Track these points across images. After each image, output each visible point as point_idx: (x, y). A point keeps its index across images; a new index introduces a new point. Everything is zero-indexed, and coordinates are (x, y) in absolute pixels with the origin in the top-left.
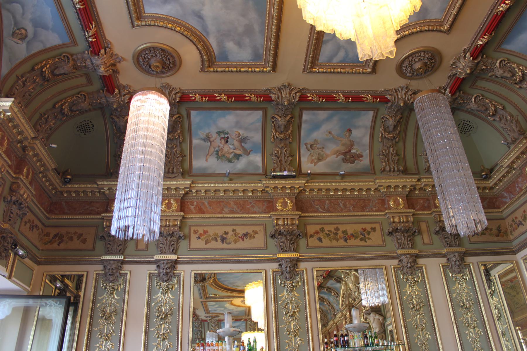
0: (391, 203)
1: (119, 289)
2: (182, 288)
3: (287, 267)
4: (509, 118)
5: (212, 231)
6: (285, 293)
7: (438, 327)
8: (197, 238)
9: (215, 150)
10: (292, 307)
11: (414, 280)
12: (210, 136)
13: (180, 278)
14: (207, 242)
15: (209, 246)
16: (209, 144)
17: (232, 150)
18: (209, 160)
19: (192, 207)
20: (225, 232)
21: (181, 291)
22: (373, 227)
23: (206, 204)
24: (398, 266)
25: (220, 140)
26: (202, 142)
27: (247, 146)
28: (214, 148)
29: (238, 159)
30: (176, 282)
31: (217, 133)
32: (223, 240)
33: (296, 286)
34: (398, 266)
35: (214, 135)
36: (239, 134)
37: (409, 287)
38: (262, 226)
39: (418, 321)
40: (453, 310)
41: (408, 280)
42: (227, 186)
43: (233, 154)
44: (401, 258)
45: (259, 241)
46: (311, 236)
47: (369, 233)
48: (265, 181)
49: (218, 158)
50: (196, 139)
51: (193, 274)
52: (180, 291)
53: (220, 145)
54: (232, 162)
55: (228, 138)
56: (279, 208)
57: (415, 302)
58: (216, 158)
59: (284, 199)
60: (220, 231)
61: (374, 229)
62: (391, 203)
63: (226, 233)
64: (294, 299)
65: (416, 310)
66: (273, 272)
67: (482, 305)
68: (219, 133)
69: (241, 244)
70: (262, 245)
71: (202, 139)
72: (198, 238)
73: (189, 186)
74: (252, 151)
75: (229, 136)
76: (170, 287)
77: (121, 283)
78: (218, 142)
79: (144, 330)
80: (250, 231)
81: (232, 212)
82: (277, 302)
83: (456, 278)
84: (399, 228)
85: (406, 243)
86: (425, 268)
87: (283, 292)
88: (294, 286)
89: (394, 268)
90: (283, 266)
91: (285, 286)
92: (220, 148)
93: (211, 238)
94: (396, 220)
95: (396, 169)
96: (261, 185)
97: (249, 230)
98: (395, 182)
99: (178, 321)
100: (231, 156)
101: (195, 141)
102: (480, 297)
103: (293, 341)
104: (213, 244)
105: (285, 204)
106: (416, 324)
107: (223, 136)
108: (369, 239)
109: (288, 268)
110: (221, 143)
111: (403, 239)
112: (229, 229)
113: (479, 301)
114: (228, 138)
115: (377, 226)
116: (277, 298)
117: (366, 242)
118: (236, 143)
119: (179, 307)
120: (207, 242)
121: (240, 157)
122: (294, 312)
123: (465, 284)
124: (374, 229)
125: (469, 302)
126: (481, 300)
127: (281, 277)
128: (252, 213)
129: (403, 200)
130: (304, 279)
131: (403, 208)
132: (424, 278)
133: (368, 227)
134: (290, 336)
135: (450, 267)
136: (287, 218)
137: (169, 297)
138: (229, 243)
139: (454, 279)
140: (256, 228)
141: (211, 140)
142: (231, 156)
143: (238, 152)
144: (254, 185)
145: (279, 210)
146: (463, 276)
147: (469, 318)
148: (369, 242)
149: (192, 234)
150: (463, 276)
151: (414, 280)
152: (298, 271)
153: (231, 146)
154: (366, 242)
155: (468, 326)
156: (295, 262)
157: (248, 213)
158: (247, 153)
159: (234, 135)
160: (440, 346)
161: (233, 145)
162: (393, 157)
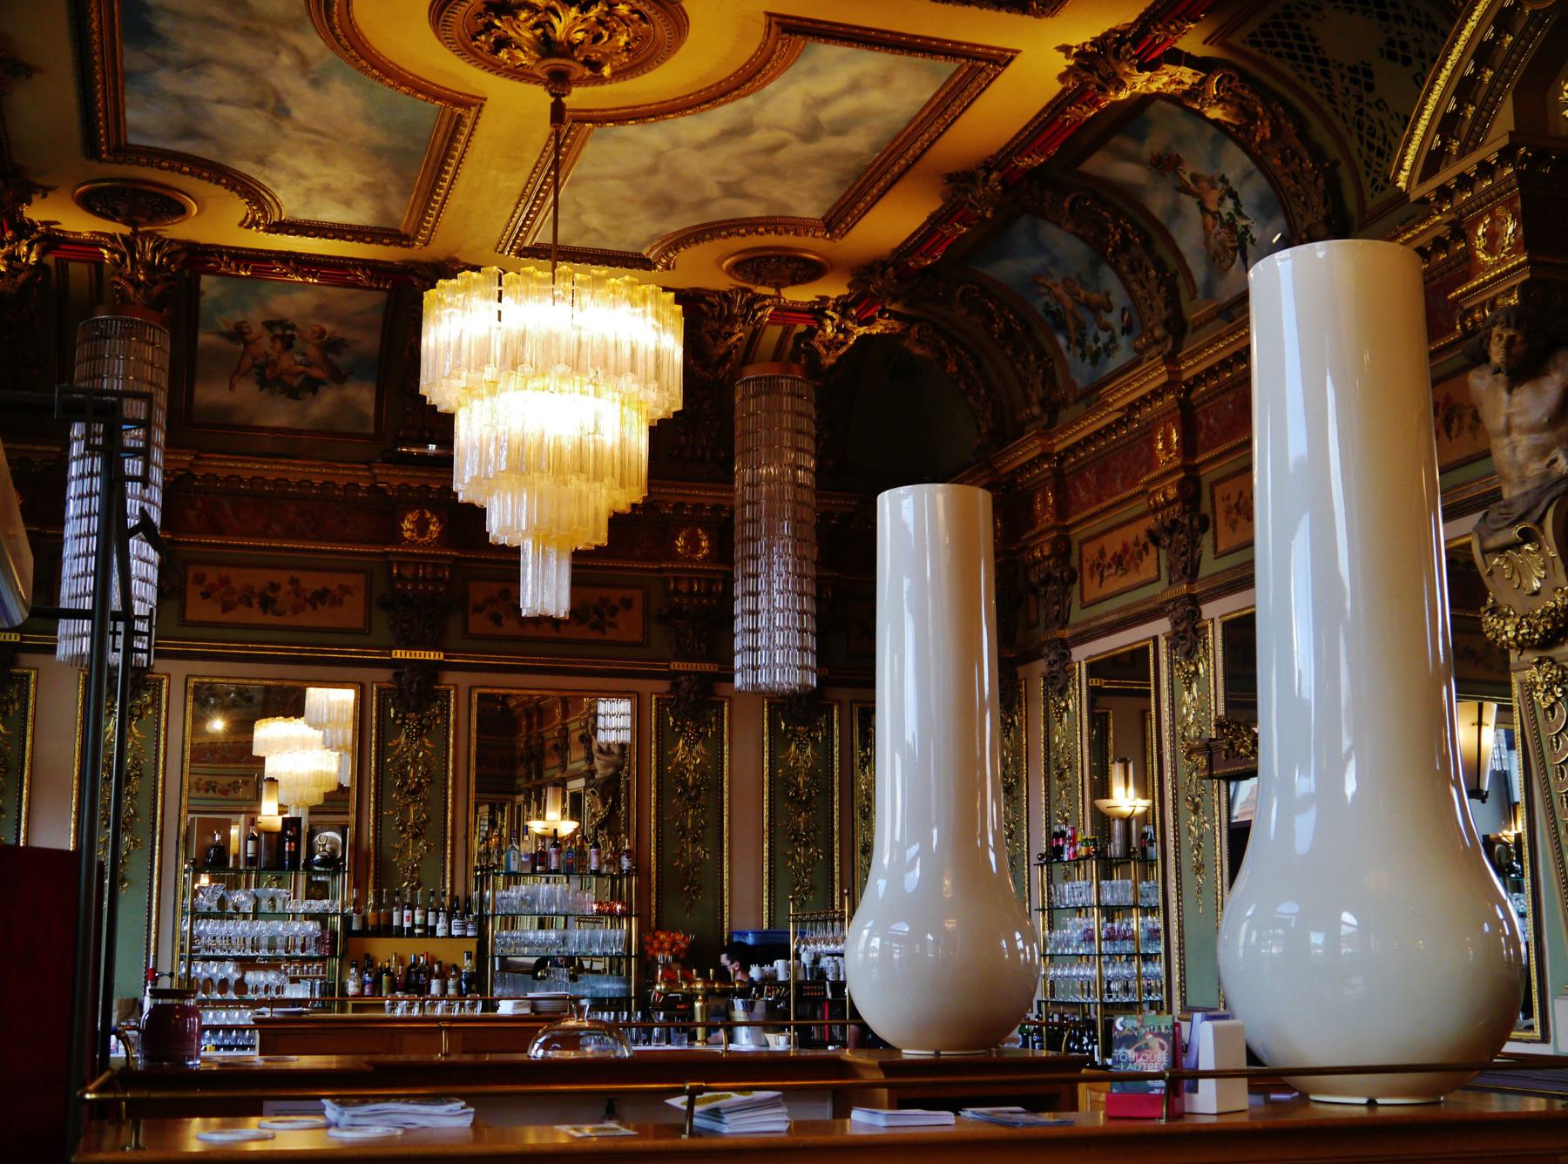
0: (680, 542)
1: (11, 712)
2: (164, 714)
3: (411, 682)
4: (983, 391)
5: (241, 579)
6: (403, 739)
7: (730, 838)
8: (202, 594)
9: (256, 362)
10: (416, 771)
11: (698, 732)
12: (246, 330)
13: (160, 691)
14: (226, 608)
15: (230, 617)
16: (242, 346)
17: (300, 368)
18: (239, 387)
19: (191, 514)
20: (272, 584)
21: (163, 724)
22: (627, 597)
23: (227, 506)
24: (668, 697)
25: (273, 339)
26: (222, 342)
27: (341, 361)
28: (254, 359)
29: (315, 391)
30: (149, 700)
31: (263, 324)
32: (267, 604)
33: (430, 727)
34: (668, 697)
35: (257, 329)
36: (323, 332)
37: (684, 745)
38: (363, 576)
39: (690, 821)
40: (770, 804)
41: (683, 730)
42: (283, 470)
43: (300, 379)
44: (678, 680)
45: (351, 612)
46: (478, 609)
47: (614, 611)
48: (379, 468)
49: (263, 383)
50: (210, 333)
51: (191, 684)
52: (159, 723)
53: (270, 351)
54: (299, 399)
55: (292, 337)
56: (407, 535)
57: (690, 781)
58: (258, 383)
59: (422, 514)
60: (258, 579)
61: (627, 604)
62: (680, 542)
63: (275, 587)
64: (421, 754)
65: (689, 798)
66: (379, 691)
67: (836, 798)
68: (269, 325)
69: (308, 618)
70: (360, 624)
71: (222, 334)
72: (206, 595)
73: (186, 466)
74: (351, 373)
75: (295, 333)
76: (137, 712)
77: (15, 696)
78: (265, 344)
79: (74, 809)
80: (333, 587)
81: (290, 534)
82: (382, 759)
83: (794, 736)
84: (684, 609)
85: (696, 645)
86: (729, 707)
87: (397, 737)
88: (423, 726)
89: (657, 700)
90: (403, 679)
91: (403, 723)
92: (271, 358)
93: (235, 598)
94: (684, 587)
95: (708, 455)
96: (367, 474)
97: (331, 582)
98: (695, 495)
99: (156, 792)
100: (296, 382)
101: (204, 338)
102: (836, 780)
103: (411, 846)
104: (240, 614)
105: (422, 526)
106: (683, 828)
107: (279, 332)
108: (613, 625)
109: (415, 686)
110: (272, 348)
111: (691, 634)
112: (282, 577)
113: (833, 788)
114: (292, 337)
115: (636, 595)
116: (383, 751)
117: (604, 633)
118: (313, 352)
119: (157, 760)
120: (226, 608)
121: (321, 388)
122: (419, 783)
123: (812, 748)
124: (627, 604)
125: (809, 791)
126: (836, 788)
127: (397, 701)
128: (342, 541)
129: (710, 539)
130: (448, 710)
131: (705, 557)
132: (723, 728)
133: (615, 595)
134: (405, 835)
135: (786, 708)
136: (424, 564)
137: (134, 735)
138: (281, 614)
139: (789, 736)
140: (350, 580)
141: (249, 337)
142: (296, 382)
143: (316, 373)
144: (351, 472)
145: (406, 539)
146: (810, 731)
147: (802, 824)
148: (611, 634)
149: (190, 587)
150: (810, 731)
151: (698, 732)
152: (438, 690)
153: (298, 358)
154: (604, 633)
155: (795, 840)
156: (432, 671)
157: (330, 540)
158: (339, 377)
159: (309, 332)
160: (726, 877)
161: (304, 354)
162: (708, 422)
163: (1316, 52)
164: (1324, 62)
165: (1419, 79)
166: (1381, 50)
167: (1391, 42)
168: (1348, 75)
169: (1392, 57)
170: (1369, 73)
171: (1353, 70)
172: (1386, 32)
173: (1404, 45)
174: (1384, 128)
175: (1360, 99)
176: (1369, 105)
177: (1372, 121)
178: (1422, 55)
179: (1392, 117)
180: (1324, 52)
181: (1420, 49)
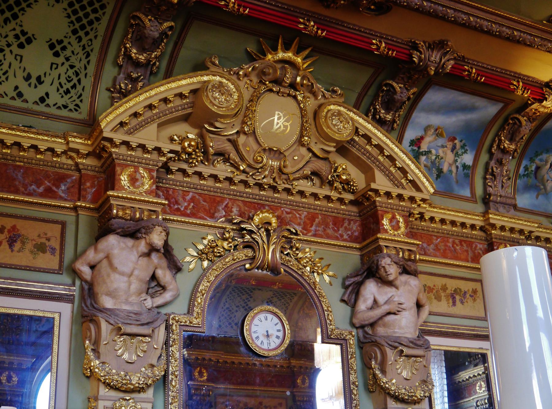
163: (19, 11)
164: (15, 16)
165: (54, 66)
166: (51, 40)
167: (60, 42)
168: (18, 31)
169: (52, 47)
170: (29, 41)
171: (24, 33)
172: (65, 37)
173: (64, 48)
174: (10, 67)
175: (9, 45)
176: (11, 52)
177: (5, 59)
178: (67, 59)
179: (20, 68)
180: (23, 14)
181: (71, 56)
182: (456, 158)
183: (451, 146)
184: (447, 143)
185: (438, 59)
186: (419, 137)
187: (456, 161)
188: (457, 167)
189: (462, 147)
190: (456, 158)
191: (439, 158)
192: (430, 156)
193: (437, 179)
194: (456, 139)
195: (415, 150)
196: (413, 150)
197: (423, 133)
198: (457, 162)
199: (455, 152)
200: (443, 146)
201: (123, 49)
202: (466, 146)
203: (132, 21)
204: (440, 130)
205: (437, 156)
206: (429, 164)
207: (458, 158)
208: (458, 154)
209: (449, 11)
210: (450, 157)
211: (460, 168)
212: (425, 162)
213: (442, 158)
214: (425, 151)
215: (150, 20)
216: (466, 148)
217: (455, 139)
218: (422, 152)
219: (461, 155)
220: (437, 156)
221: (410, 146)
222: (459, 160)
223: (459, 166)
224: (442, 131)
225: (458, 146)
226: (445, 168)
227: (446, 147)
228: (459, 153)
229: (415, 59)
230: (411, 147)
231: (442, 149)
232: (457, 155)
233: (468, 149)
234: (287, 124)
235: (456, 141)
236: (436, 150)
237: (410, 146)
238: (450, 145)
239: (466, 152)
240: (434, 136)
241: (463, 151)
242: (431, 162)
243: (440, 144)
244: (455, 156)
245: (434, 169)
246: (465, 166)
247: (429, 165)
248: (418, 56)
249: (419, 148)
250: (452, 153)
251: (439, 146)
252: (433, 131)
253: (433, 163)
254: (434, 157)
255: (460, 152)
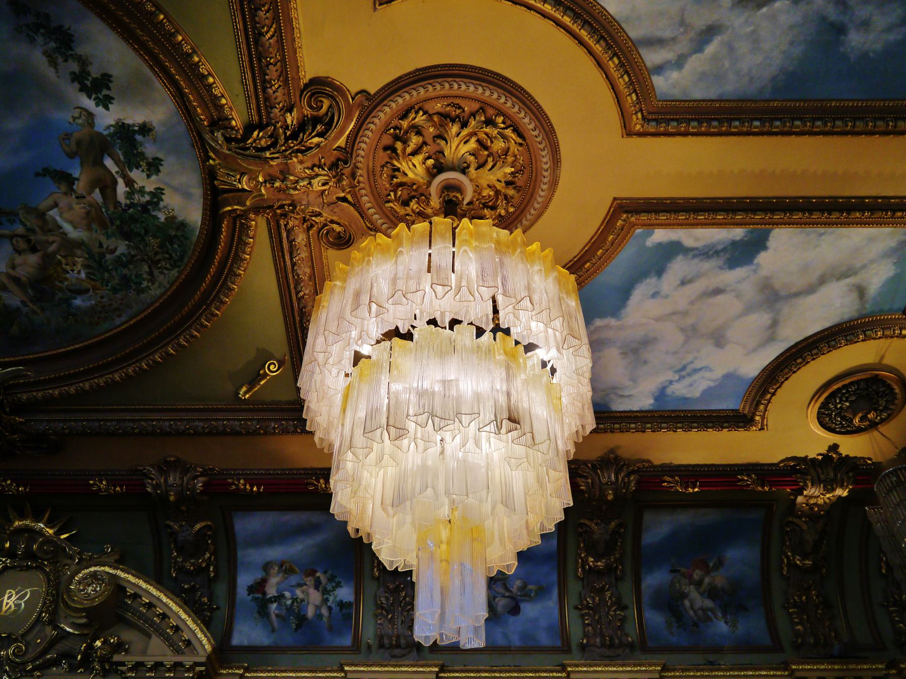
182: (325, 597)
183: (312, 582)
184: (305, 579)
185: (178, 481)
186: (260, 580)
187: (327, 600)
188: (330, 608)
189: (331, 579)
190: (325, 597)
191: (297, 602)
192: (284, 601)
193: (296, 630)
194: (317, 572)
195: (259, 598)
196: (255, 599)
197: (264, 574)
198: (328, 601)
199: (320, 589)
200: (300, 585)
201: (580, 561)
202: (336, 577)
203: (580, 530)
204: (288, 565)
205: (294, 600)
206: (284, 612)
207: (328, 596)
208: (326, 591)
209: (109, 424)
210: (315, 597)
211: (336, 609)
212: (276, 611)
213: (302, 600)
214: (274, 597)
215: (596, 524)
216: (337, 580)
217: (314, 572)
218: (271, 598)
219: (332, 591)
220: (294, 600)
221: (249, 595)
222: (331, 599)
223: (333, 606)
224: (290, 566)
225: (323, 579)
226: (310, 612)
227: (306, 585)
228: (328, 589)
229: (582, 488)
230: (252, 595)
231: (300, 588)
232: (325, 592)
233: (340, 580)
234: (20, 602)
235: (318, 574)
236: (293, 593)
237: (249, 595)
238: (310, 581)
239: (338, 585)
240: (281, 575)
241: (334, 584)
242: (287, 609)
243: (294, 583)
244: (323, 594)
245: (291, 618)
246: (342, 605)
247: (284, 614)
248: (583, 482)
249: (264, 594)
250: (316, 591)
251: (293, 586)
252: (276, 568)
253: (290, 609)
254: (289, 602)
255: (329, 587)
